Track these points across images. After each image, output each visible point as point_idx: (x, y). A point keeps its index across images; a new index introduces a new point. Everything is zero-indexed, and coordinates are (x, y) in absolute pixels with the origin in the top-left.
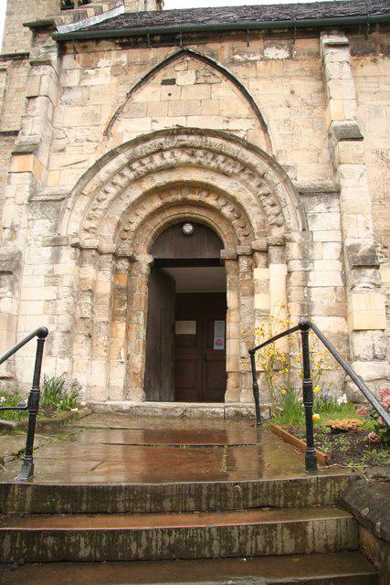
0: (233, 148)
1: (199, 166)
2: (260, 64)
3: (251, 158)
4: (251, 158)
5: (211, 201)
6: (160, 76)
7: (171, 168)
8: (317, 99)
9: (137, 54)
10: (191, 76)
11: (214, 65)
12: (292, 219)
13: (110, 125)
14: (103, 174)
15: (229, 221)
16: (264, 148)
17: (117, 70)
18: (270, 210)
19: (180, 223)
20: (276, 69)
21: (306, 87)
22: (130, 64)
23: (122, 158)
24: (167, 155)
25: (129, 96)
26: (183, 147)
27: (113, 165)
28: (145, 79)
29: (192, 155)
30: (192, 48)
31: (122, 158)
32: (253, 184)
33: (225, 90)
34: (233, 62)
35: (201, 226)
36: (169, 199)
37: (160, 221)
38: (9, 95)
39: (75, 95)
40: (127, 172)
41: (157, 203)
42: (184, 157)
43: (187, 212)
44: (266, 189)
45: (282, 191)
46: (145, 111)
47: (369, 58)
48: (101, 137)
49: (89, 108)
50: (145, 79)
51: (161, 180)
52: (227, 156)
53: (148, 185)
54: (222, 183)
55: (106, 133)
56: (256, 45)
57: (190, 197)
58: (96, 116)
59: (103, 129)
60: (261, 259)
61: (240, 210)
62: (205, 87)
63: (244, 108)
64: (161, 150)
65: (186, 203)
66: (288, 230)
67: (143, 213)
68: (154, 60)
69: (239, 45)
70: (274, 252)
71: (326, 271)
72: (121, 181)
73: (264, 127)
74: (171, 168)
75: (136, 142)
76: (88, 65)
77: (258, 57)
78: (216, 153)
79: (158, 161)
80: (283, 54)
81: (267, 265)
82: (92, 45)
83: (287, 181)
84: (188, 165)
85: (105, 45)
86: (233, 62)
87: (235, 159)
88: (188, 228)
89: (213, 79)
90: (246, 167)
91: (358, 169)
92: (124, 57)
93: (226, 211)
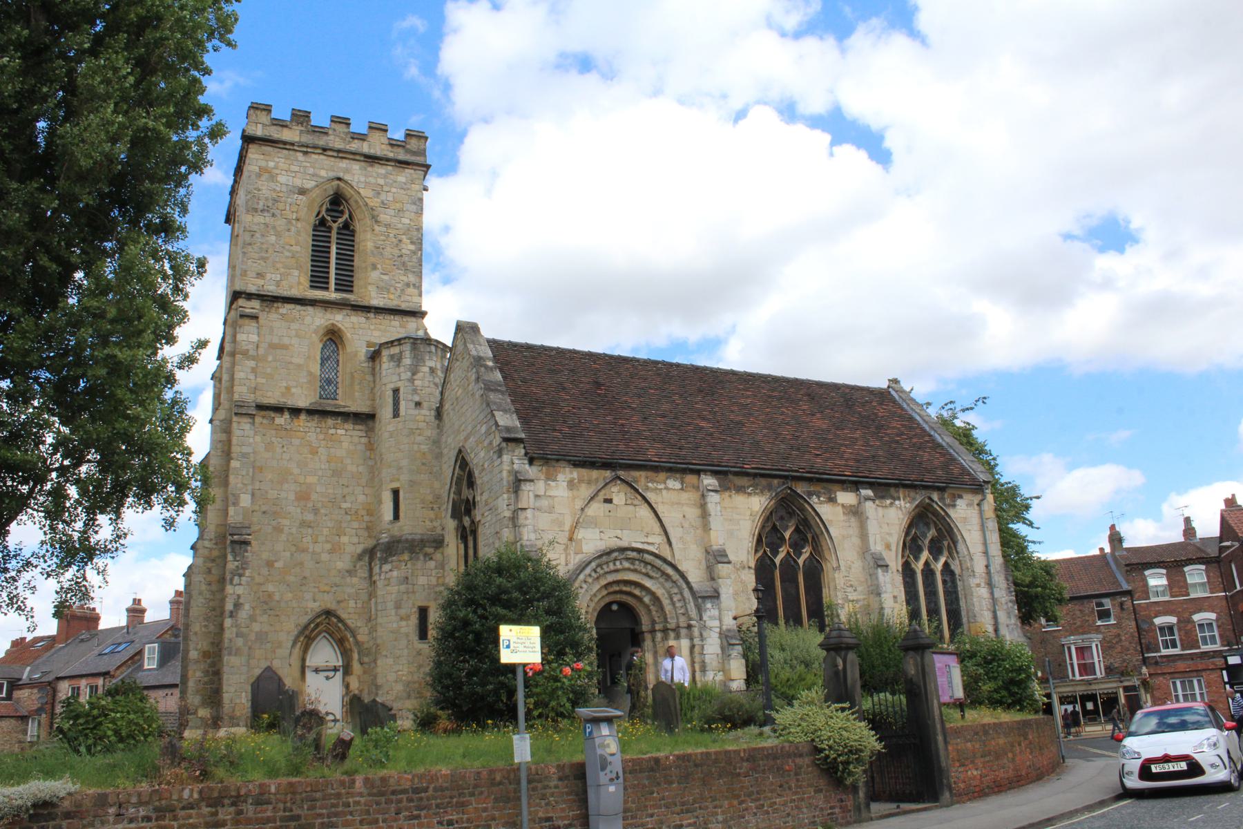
0: (658, 563)
1: (635, 571)
2: (664, 492)
3: (670, 571)
4: (670, 571)
5: (637, 592)
6: (601, 496)
7: (617, 571)
8: (698, 522)
9: (584, 472)
10: (622, 495)
11: (636, 490)
12: (693, 612)
13: (572, 532)
14: (582, 577)
15: (647, 606)
16: (669, 559)
17: (571, 485)
18: (678, 605)
19: (610, 604)
20: (672, 496)
21: (693, 513)
22: (581, 481)
23: (593, 565)
24: (618, 563)
25: (582, 509)
26: (627, 559)
27: (588, 571)
28: (592, 498)
29: (633, 564)
30: (621, 473)
31: (593, 565)
32: (669, 585)
33: (644, 511)
34: (647, 489)
35: (622, 605)
36: (611, 590)
37: (603, 604)
38: (261, 351)
39: (544, 503)
40: (593, 574)
41: (605, 592)
42: (626, 565)
43: (618, 597)
44: (676, 590)
45: (687, 593)
46: (594, 523)
47: (727, 494)
48: (565, 541)
49: (554, 516)
50: (592, 498)
51: (610, 578)
52: (653, 566)
53: (603, 582)
54: (648, 583)
55: (571, 539)
56: (662, 475)
57: (624, 589)
58: (561, 524)
59: (567, 534)
60: (672, 635)
61: (656, 599)
62: (631, 508)
63: (657, 528)
64: (615, 560)
65: (621, 592)
66: (691, 619)
67: (596, 599)
68: (597, 480)
69: (650, 474)
70: (683, 632)
71: (712, 646)
72: (590, 580)
73: (670, 544)
74: (617, 571)
75: (600, 556)
76: (550, 478)
77: (662, 486)
78: (647, 563)
79: (612, 567)
80: (678, 485)
81: (678, 637)
82: (554, 463)
83: (688, 583)
84: (629, 569)
85: (562, 464)
86: (647, 489)
87: (659, 569)
88: (615, 607)
89: (636, 502)
90: (664, 573)
91: (728, 581)
92: (575, 474)
93: (647, 599)
